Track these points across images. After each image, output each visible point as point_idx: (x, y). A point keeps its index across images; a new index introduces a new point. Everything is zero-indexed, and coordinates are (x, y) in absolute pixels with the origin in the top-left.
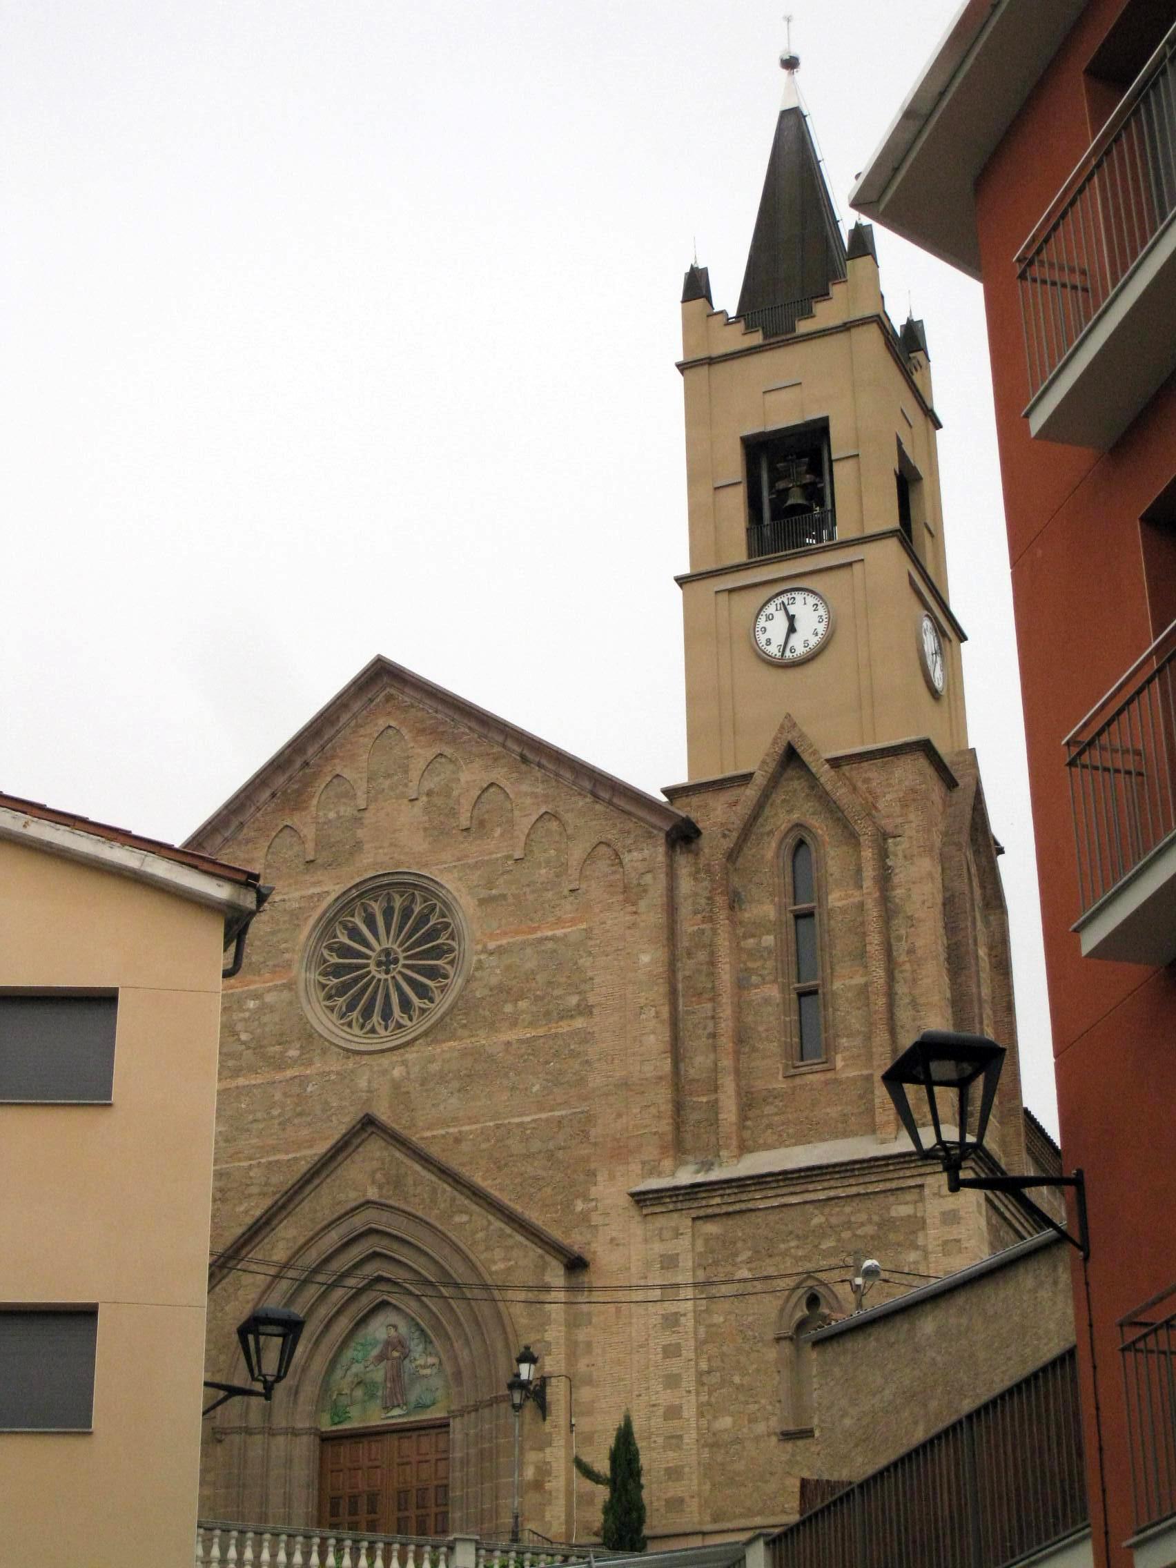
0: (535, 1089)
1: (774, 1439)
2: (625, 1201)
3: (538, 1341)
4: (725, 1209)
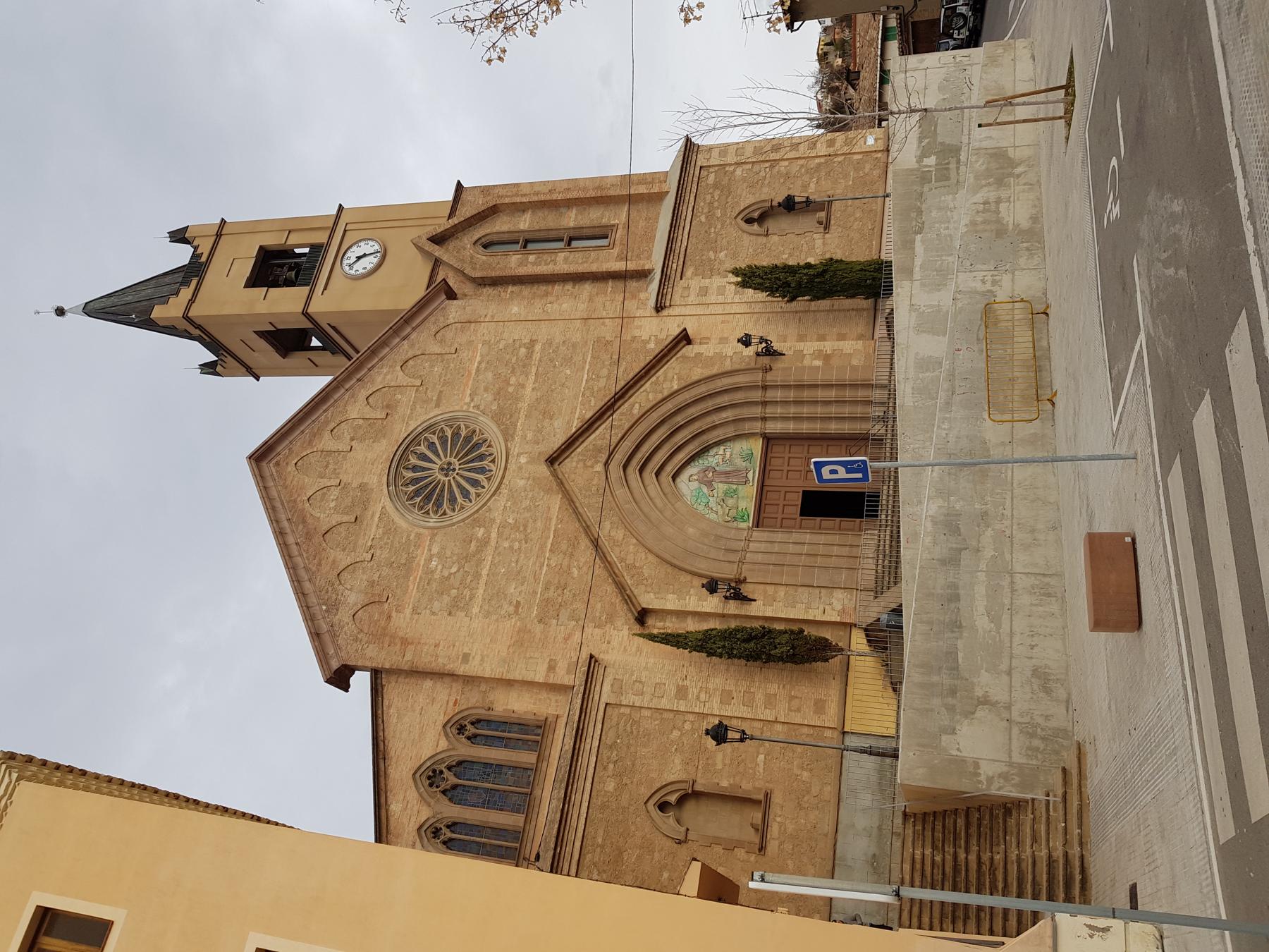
0: (568, 372)
1: (827, 236)
2: (655, 321)
4: (681, 262)
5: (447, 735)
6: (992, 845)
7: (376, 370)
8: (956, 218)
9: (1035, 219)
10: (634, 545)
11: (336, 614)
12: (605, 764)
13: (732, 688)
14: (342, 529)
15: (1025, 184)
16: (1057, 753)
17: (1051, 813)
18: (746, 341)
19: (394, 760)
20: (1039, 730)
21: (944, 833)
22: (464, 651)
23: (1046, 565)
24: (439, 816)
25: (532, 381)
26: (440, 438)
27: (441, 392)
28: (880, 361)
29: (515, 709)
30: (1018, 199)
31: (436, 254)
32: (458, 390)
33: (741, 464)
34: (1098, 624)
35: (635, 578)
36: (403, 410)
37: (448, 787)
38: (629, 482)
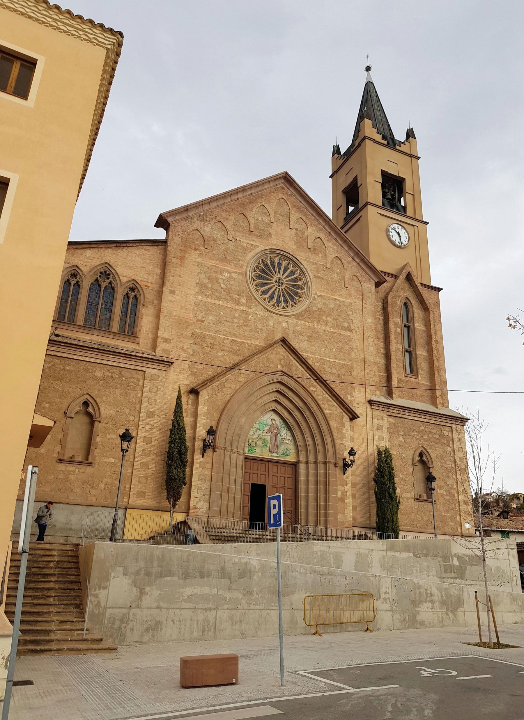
0: (334, 350)
1: (413, 500)
2: (363, 400)
3: (341, 444)
4: (397, 415)
5: (129, 281)
6: (58, 596)
7: (335, 243)
8: (422, 576)
9: (422, 624)
10: (236, 388)
11: (198, 220)
12: (111, 371)
13: (153, 444)
14: (246, 224)
15: (442, 618)
16: (111, 636)
17: (76, 632)
18: (352, 452)
19: (115, 252)
20: (125, 625)
21: (66, 568)
22: (176, 291)
23: (221, 630)
24: (83, 277)
25: (329, 330)
26: (297, 278)
27: (323, 279)
28: (340, 531)
29: (143, 320)
30: (434, 614)
31: (401, 276)
32: (324, 288)
33: (282, 449)
34: (185, 662)
35: (217, 388)
36: (313, 258)
37: (100, 282)
38: (271, 385)
